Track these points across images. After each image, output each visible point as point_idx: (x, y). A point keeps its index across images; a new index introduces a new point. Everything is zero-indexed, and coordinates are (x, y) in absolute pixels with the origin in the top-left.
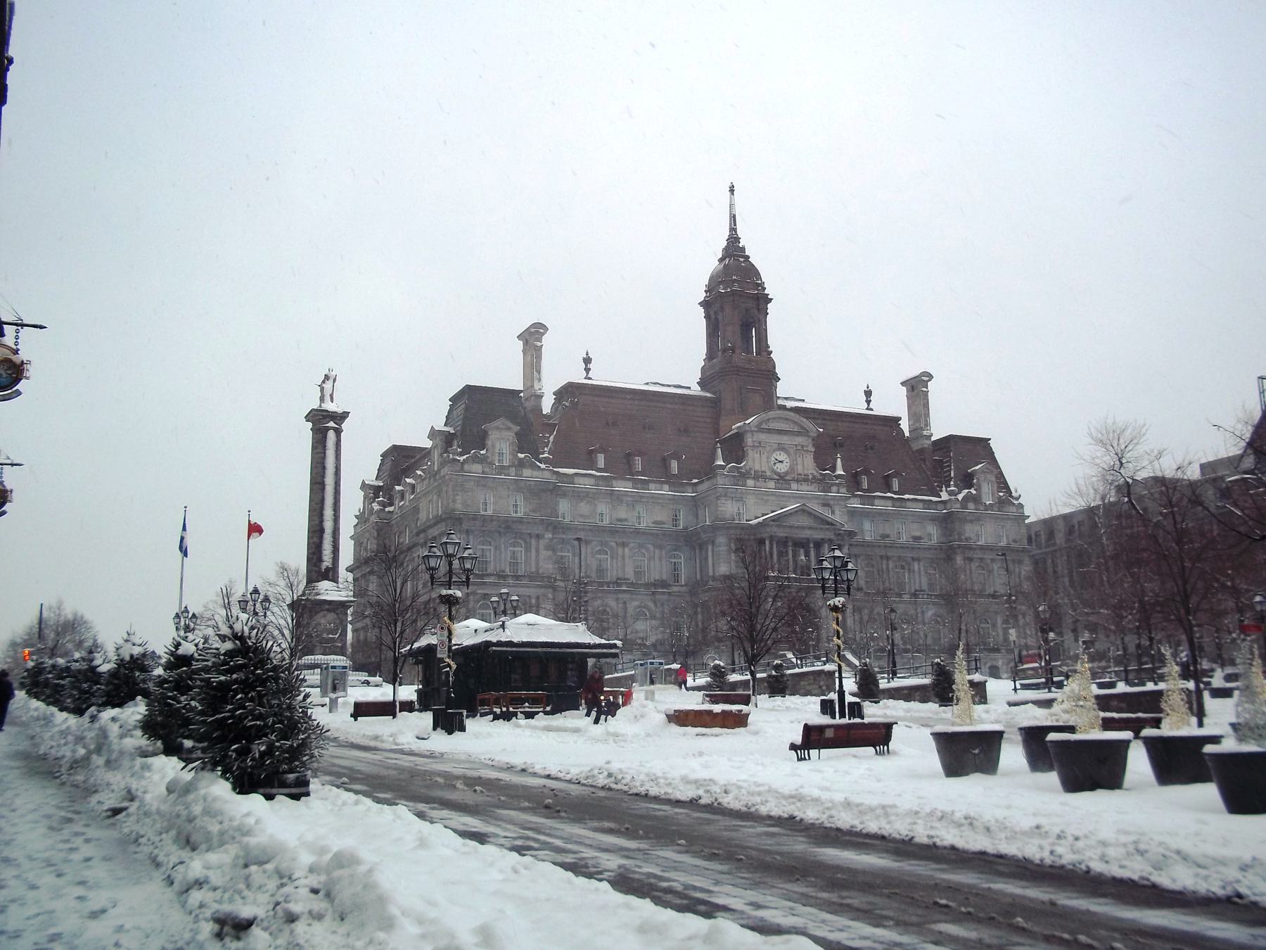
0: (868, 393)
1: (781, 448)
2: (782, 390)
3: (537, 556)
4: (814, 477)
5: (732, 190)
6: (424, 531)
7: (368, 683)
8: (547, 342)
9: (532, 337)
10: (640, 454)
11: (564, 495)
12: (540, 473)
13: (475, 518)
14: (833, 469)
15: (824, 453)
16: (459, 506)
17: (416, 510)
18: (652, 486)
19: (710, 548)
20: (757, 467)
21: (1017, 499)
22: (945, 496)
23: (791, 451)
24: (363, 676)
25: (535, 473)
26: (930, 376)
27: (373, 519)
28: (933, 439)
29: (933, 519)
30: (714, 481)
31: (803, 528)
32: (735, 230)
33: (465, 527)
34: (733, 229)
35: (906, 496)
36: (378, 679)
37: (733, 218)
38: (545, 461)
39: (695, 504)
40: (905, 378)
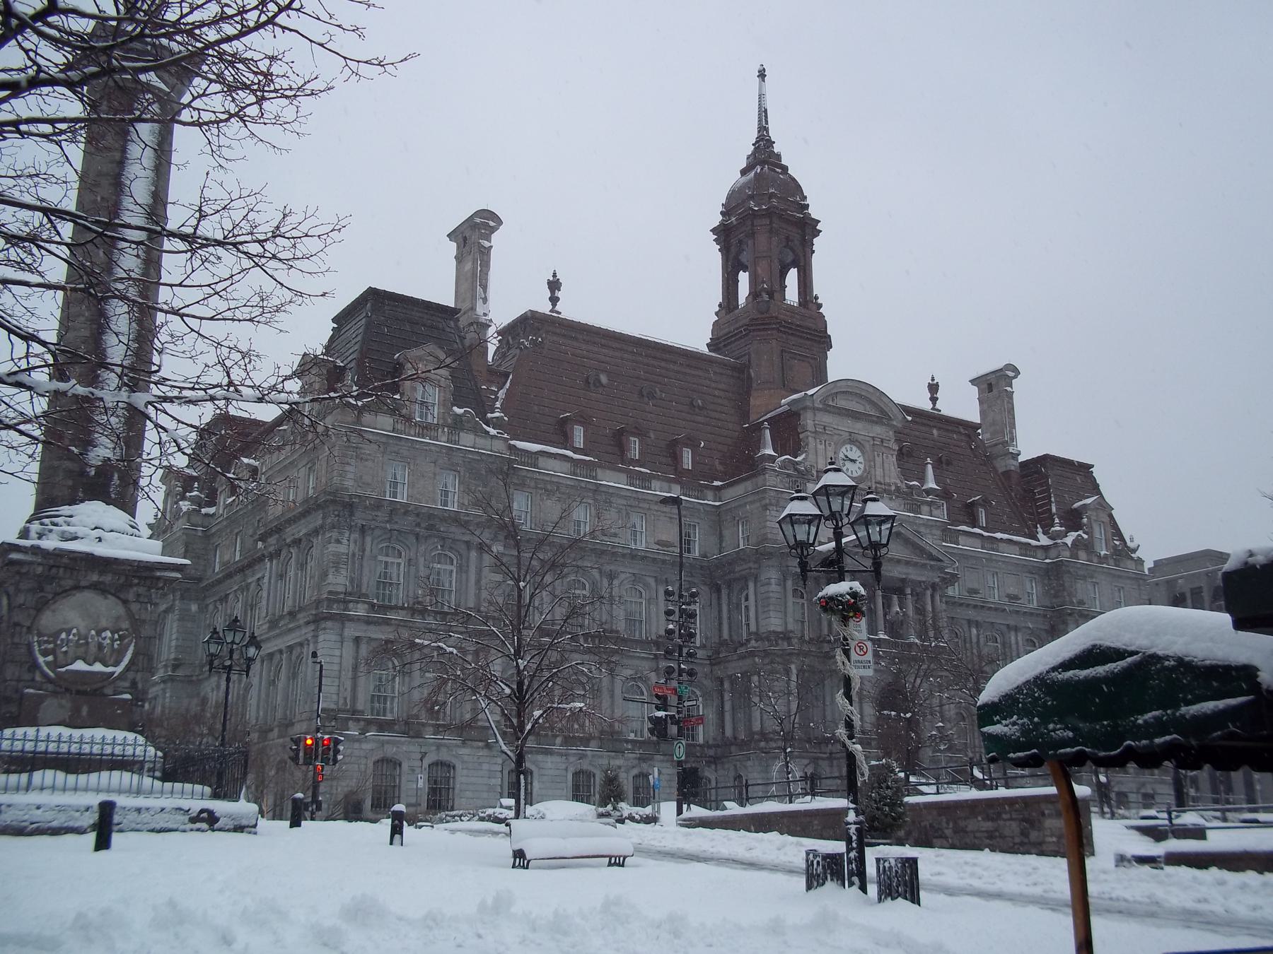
0: (933, 388)
1: (852, 441)
2: (839, 366)
3: (478, 581)
4: (898, 488)
5: (762, 75)
6: (278, 530)
7: (210, 820)
8: (498, 241)
9: (474, 236)
10: (640, 433)
11: (522, 486)
12: (489, 442)
13: (378, 505)
14: (922, 479)
15: (908, 458)
16: (349, 483)
17: (260, 502)
18: (655, 484)
19: (751, 585)
21: (1134, 551)
22: (1044, 540)
23: (867, 446)
24: (195, 798)
25: (481, 441)
26: (1017, 372)
27: (182, 524)
28: (1021, 459)
29: (1032, 570)
30: (760, 479)
31: (899, 561)
32: (767, 130)
33: (359, 518)
34: (763, 129)
35: (999, 535)
36: (243, 807)
37: (763, 114)
38: (496, 423)
39: (718, 518)
40: (975, 375)
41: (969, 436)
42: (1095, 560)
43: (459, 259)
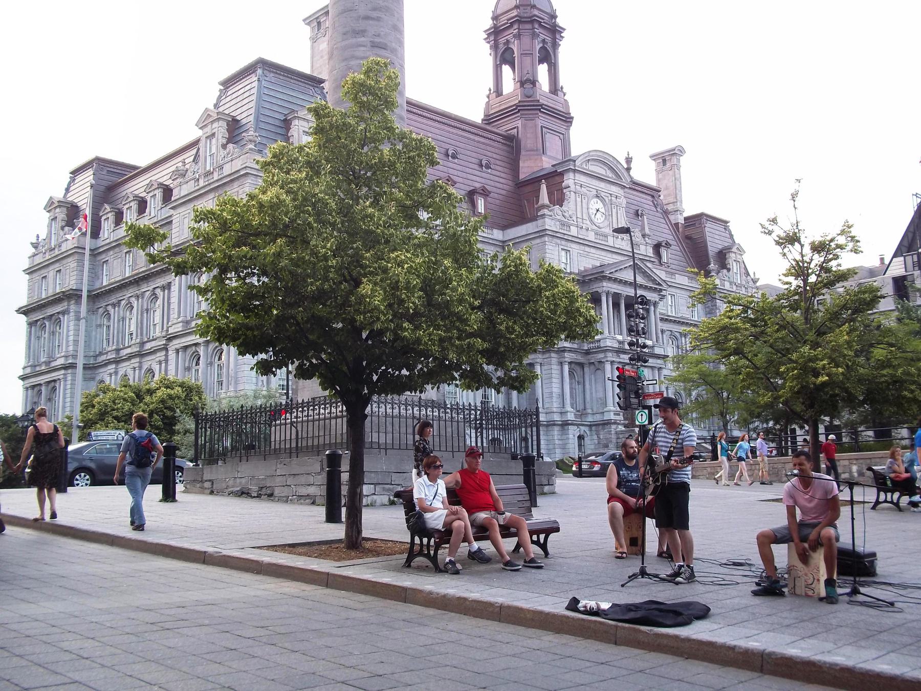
1: (597, 197)
20: (579, 215)
28: (686, 215)
30: (540, 222)
41: (653, 197)
42: (734, 287)
43: (314, 40)
